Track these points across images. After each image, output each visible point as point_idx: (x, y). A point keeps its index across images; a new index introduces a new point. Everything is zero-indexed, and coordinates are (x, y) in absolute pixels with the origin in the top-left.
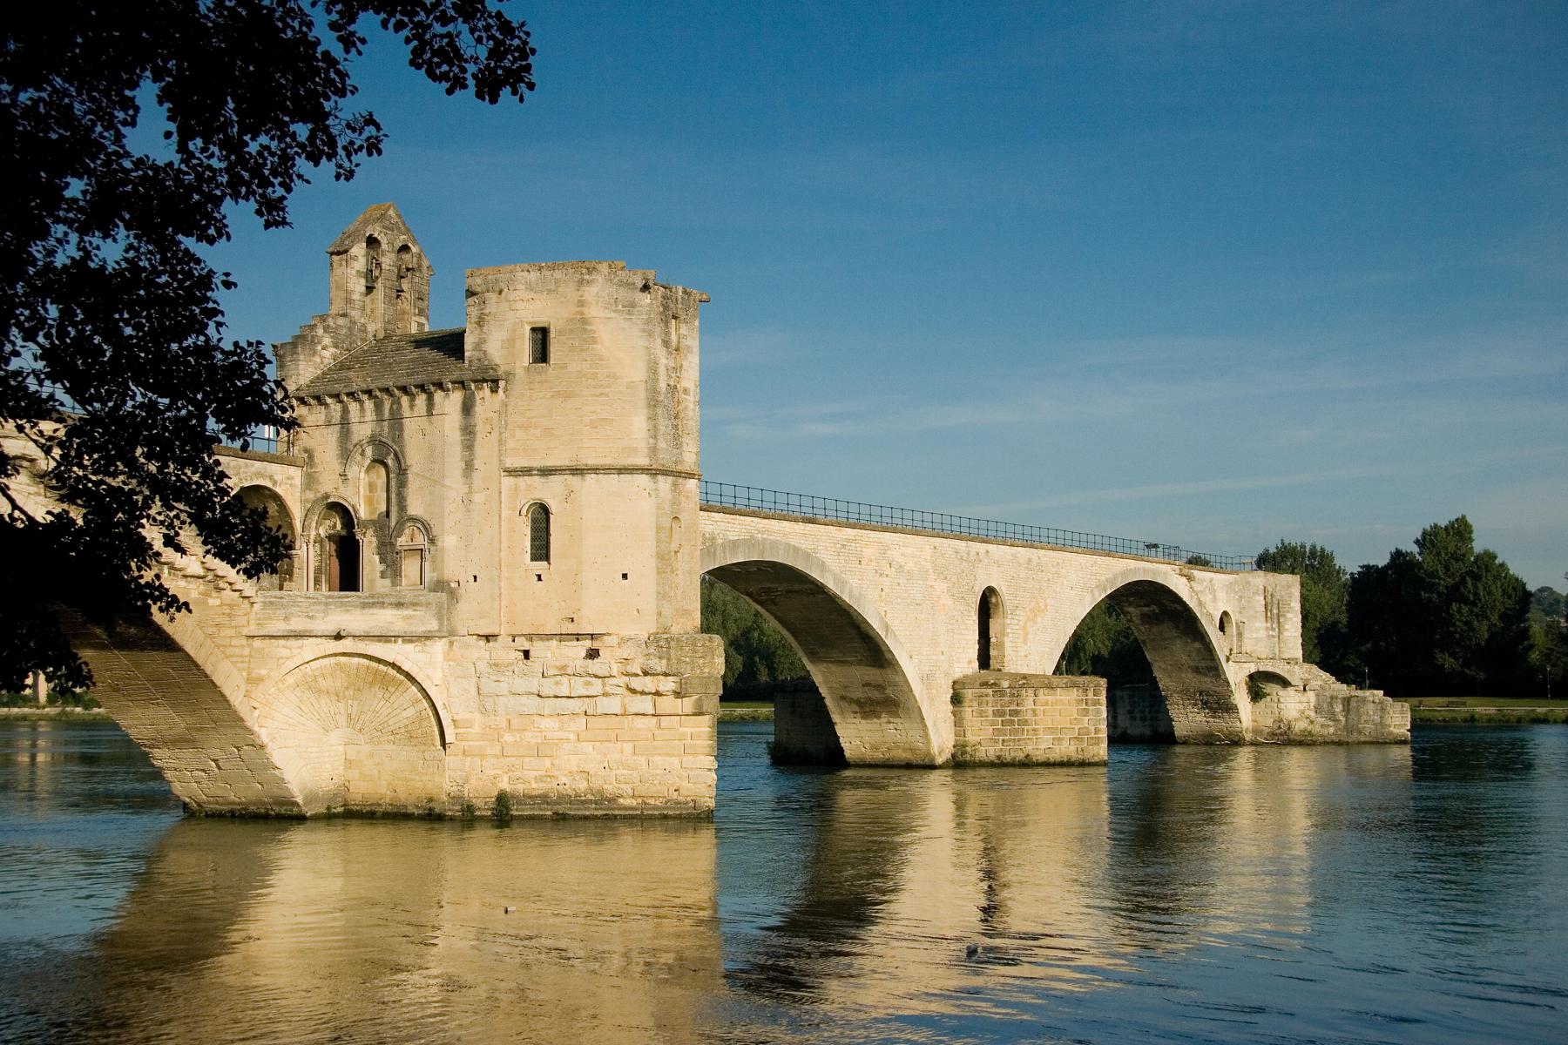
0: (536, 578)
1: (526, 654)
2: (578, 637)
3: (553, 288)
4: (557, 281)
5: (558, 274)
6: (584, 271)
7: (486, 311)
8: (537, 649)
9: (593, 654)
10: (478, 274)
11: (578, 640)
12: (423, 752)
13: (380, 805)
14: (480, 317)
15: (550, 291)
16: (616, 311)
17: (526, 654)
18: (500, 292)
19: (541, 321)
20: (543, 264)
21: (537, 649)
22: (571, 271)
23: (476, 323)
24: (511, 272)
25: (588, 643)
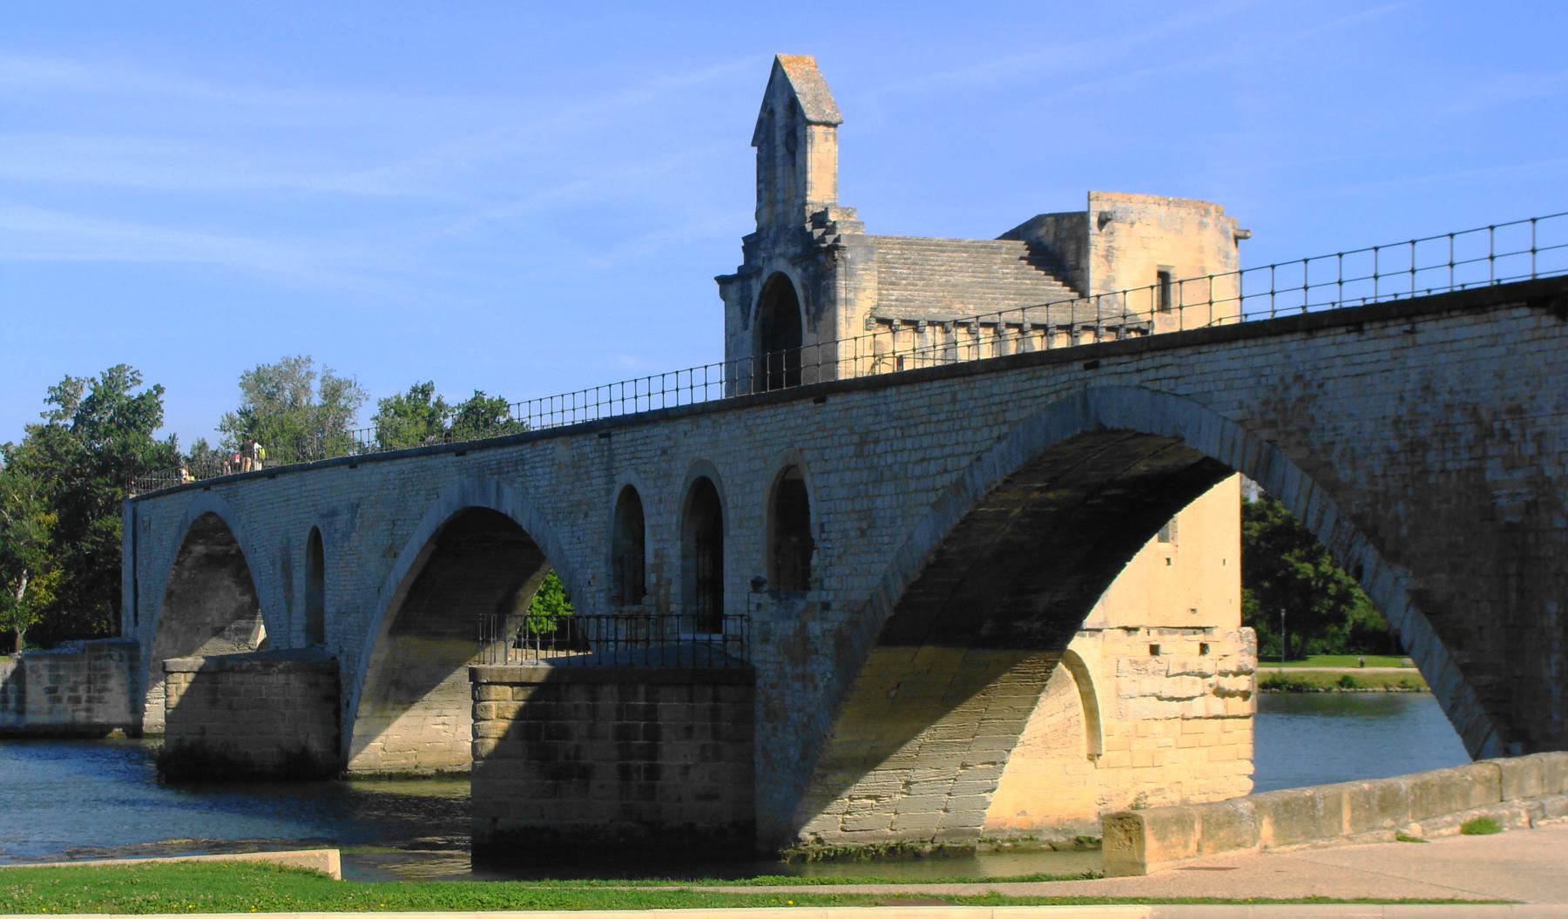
0: (1166, 562)
1: (1154, 650)
2: (1196, 629)
3: (1178, 227)
4: (1182, 220)
5: (1183, 212)
6: (1203, 213)
7: (1115, 244)
8: (1168, 644)
9: (1204, 648)
10: (1105, 197)
11: (1195, 633)
12: (1065, 766)
13: (1004, 831)
14: (1107, 250)
15: (1176, 230)
16: (1220, 262)
17: (1154, 650)
18: (1132, 224)
19: (1165, 262)
20: (1171, 199)
21: (1168, 644)
22: (1194, 210)
23: (1102, 256)
24: (1144, 202)
25: (1201, 637)
